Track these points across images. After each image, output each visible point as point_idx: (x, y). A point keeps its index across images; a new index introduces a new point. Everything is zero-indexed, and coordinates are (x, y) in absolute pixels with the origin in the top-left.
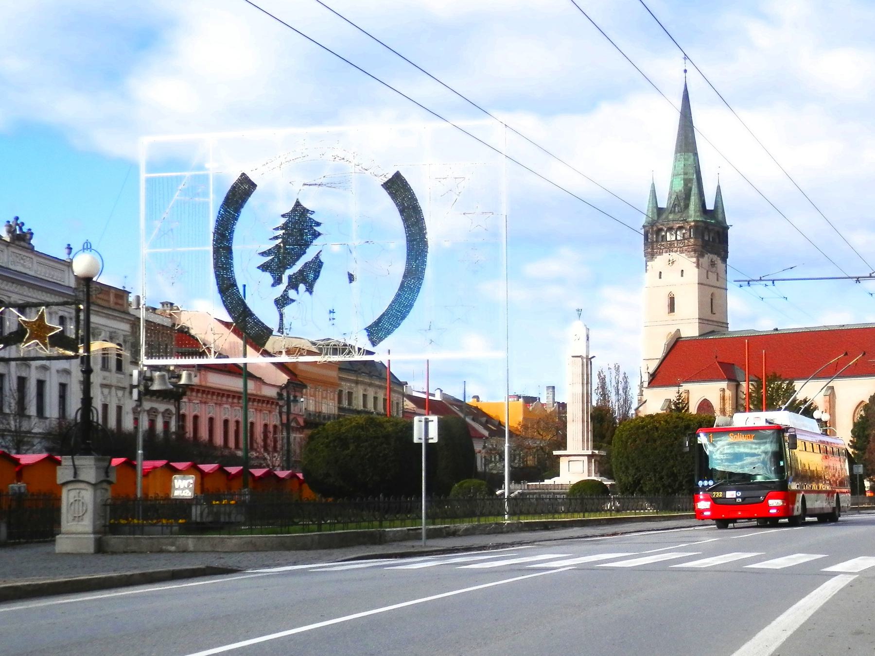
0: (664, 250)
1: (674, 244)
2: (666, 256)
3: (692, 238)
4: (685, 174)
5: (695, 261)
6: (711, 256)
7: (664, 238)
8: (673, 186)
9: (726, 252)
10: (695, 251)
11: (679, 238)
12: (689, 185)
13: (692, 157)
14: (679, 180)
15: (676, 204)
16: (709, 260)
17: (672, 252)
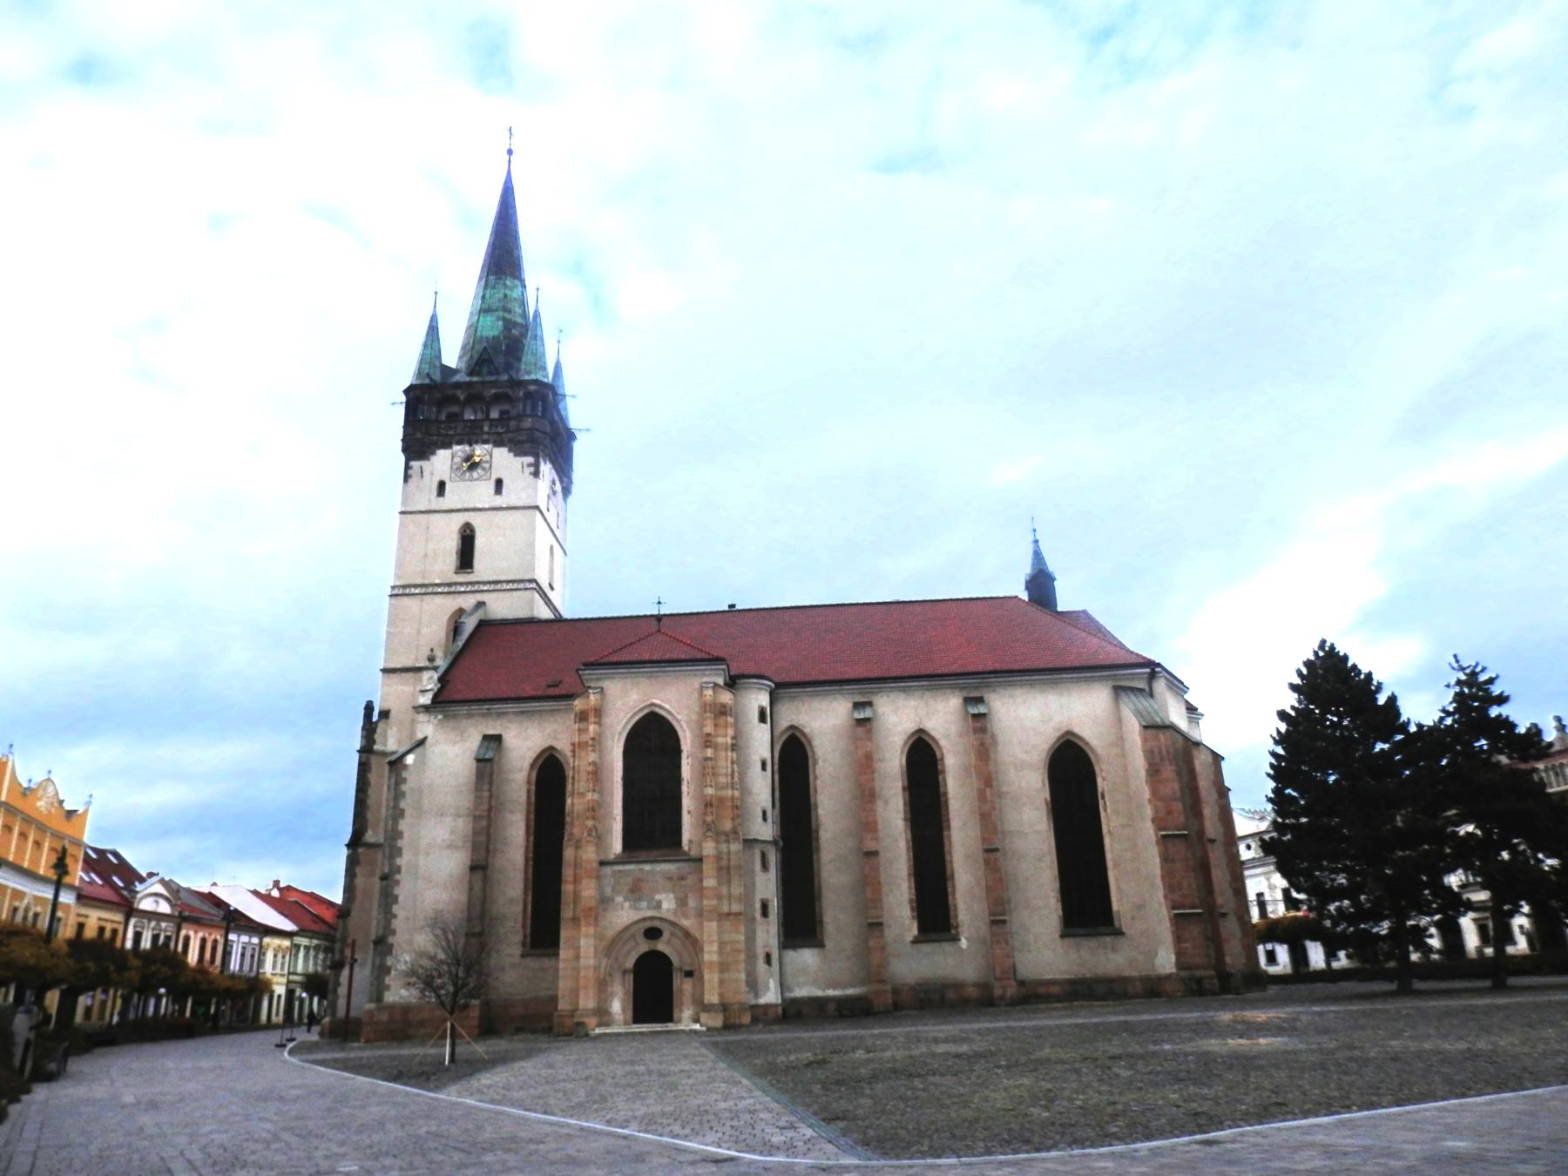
0: (457, 438)
1: (482, 427)
2: (460, 450)
3: (530, 416)
6: (553, 471)
8: (479, 329)
9: (570, 482)
11: (494, 414)
12: (514, 332)
13: (520, 289)
14: (494, 319)
15: (486, 360)
17: (477, 443)
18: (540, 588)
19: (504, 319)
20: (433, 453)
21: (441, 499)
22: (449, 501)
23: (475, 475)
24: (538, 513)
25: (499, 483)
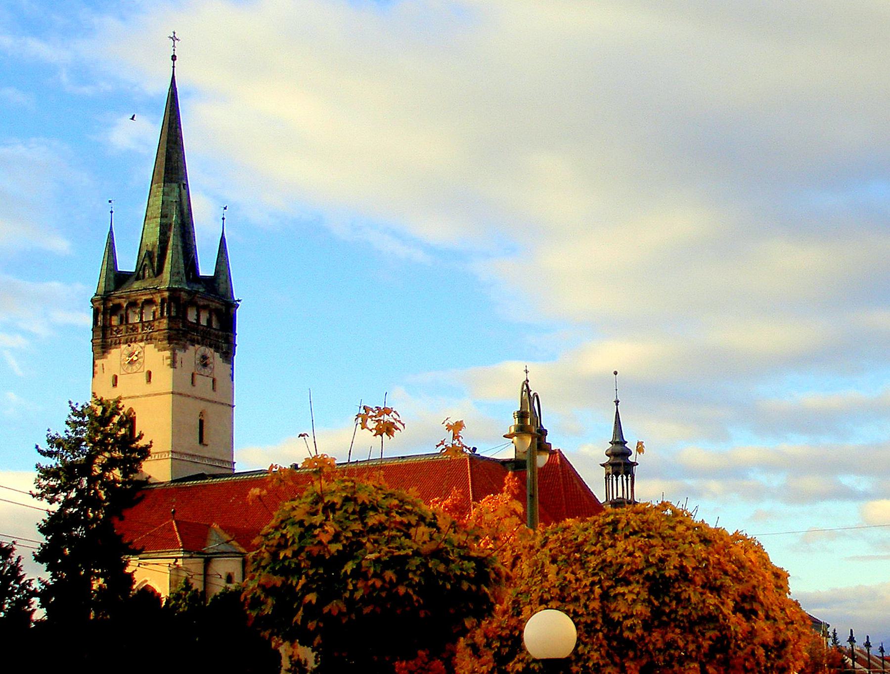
4: (162, 217)
5: (169, 355)
6: (203, 348)
7: (124, 320)
10: (170, 339)
11: (148, 317)
13: (177, 190)
14: (154, 225)
16: (198, 356)
17: (135, 342)
18: (181, 454)
19: (161, 225)
20: (110, 353)
21: (115, 389)
23: (134, 367)
25: (149, 373)
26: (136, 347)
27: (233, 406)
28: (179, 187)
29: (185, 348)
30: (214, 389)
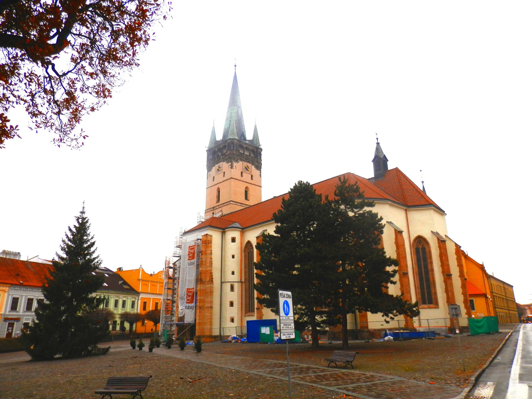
6: (246, 164)
10: (230, 158)
18: (236, 202)
20: (212, 169)
22: (216, 182)
24: (232, 180)
25: (224, 173)
26: (220, 164)
27: (261, 187)
28: (237, 107)
29: (237, 161)
30: (252, 179)
